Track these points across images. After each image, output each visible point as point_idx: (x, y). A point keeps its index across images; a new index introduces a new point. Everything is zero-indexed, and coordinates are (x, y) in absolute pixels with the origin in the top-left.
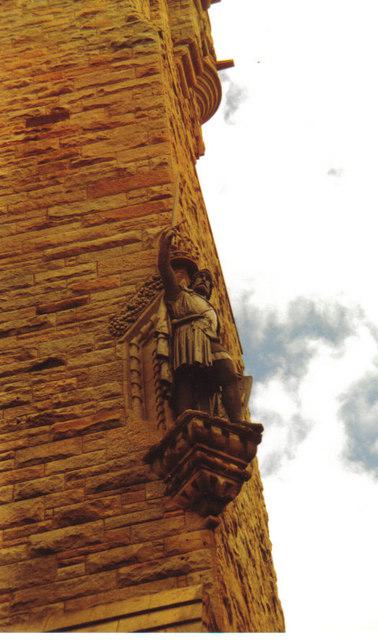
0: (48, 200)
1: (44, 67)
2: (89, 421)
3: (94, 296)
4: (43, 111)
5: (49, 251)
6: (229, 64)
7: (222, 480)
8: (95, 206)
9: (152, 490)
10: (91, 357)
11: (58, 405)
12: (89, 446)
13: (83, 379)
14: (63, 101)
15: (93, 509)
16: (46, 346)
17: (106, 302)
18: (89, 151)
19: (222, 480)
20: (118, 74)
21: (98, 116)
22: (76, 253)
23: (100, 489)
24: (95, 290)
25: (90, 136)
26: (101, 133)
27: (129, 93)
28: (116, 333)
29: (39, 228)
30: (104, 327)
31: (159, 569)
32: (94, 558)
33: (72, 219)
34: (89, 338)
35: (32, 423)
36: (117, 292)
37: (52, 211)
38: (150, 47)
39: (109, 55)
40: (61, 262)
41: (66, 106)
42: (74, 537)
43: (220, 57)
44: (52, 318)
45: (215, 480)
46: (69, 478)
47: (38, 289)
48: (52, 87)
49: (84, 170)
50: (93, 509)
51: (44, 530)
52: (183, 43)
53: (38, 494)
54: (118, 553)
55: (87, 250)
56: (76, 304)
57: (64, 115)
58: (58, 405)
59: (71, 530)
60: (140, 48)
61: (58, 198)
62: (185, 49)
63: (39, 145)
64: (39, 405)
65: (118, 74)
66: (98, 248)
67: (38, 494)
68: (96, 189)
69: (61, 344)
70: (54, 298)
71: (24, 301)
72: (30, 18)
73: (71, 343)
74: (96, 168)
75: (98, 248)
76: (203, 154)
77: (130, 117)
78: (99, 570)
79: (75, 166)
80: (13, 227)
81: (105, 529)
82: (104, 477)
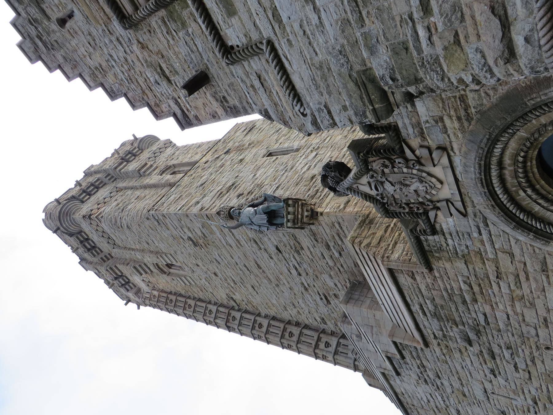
0: (221, 244)
1: (176, 241)
2: (294, 241)
3: (250, 236)
4: (191, 242)
5: (239, 246)
6: (134, 136)
7: (306, 214)
8: (218, 234)
9: (312, 227)
10: (272, 239)
11: (292, 248)
12: (303, 241)
13: (281, 241)
14: (186, 238)
15: (324, 243)
16: (272, 250)
17: (252, 235)
18: (200, 234)
19: (306, 214)
20: (169, 224)
21: (186, 230)
22: (237, 240)
23: (317, 241)
24: (248, 236)
25: (194, 233)
26: (192, 230)
27: (174, 222)
28: (261, 232)
29: (232, 247)
30: (261, 235)
31: (340, 229)
32: (340, 243)
33: (225, 240)
34: (266, 239)
35: (299, 254)
36: (247, 231)
37: (225, 244)
38: (155, 215)
39: (163, 226)
40: (242, 243)
41: (187, 237)
42: (334, 248)
43: (132, 138)
44: (262, 247)
45: (307, 216)
46: (315, 247)
47: (253, 249)
48: (181, 240)
49: (206, 235)
50: (324, 243)
51: (333, 254)
52: (139, 173)
53: (322, 254)
54: (337, 238)
55: (235, 237)
56: (255, 241)
57: (190, 239)
58: (292, 248)
59: (332, 248)
60: (157, 218)
61: (220, 243)
62: (141, 174)
63: (203, 245)
64: (293, 252)
65: (169, 224)
66: (233, 234)
67: (322, 254)
68: (212, 232)
69: (270, 246)
70: (254, 245)
71: (258, 253)
72: (160, 242)
73: (269, 243)
74: (204, 232)
75: (233, 234)
76: (169, 140)
77: (182, 222)
78: (343, 242)
79: (206, 237)
80: (234, 253)
81: (330, 241)
82: (313, 240)
